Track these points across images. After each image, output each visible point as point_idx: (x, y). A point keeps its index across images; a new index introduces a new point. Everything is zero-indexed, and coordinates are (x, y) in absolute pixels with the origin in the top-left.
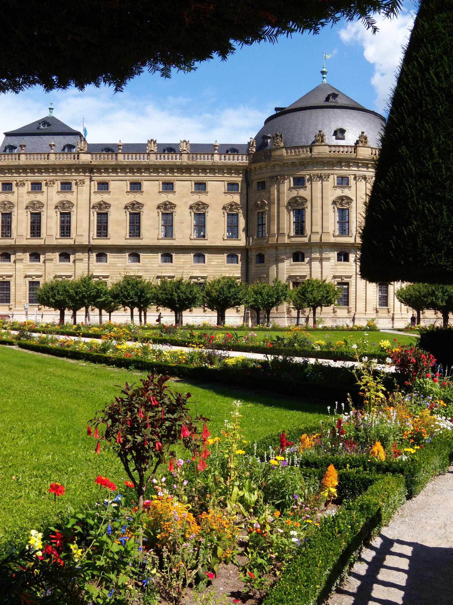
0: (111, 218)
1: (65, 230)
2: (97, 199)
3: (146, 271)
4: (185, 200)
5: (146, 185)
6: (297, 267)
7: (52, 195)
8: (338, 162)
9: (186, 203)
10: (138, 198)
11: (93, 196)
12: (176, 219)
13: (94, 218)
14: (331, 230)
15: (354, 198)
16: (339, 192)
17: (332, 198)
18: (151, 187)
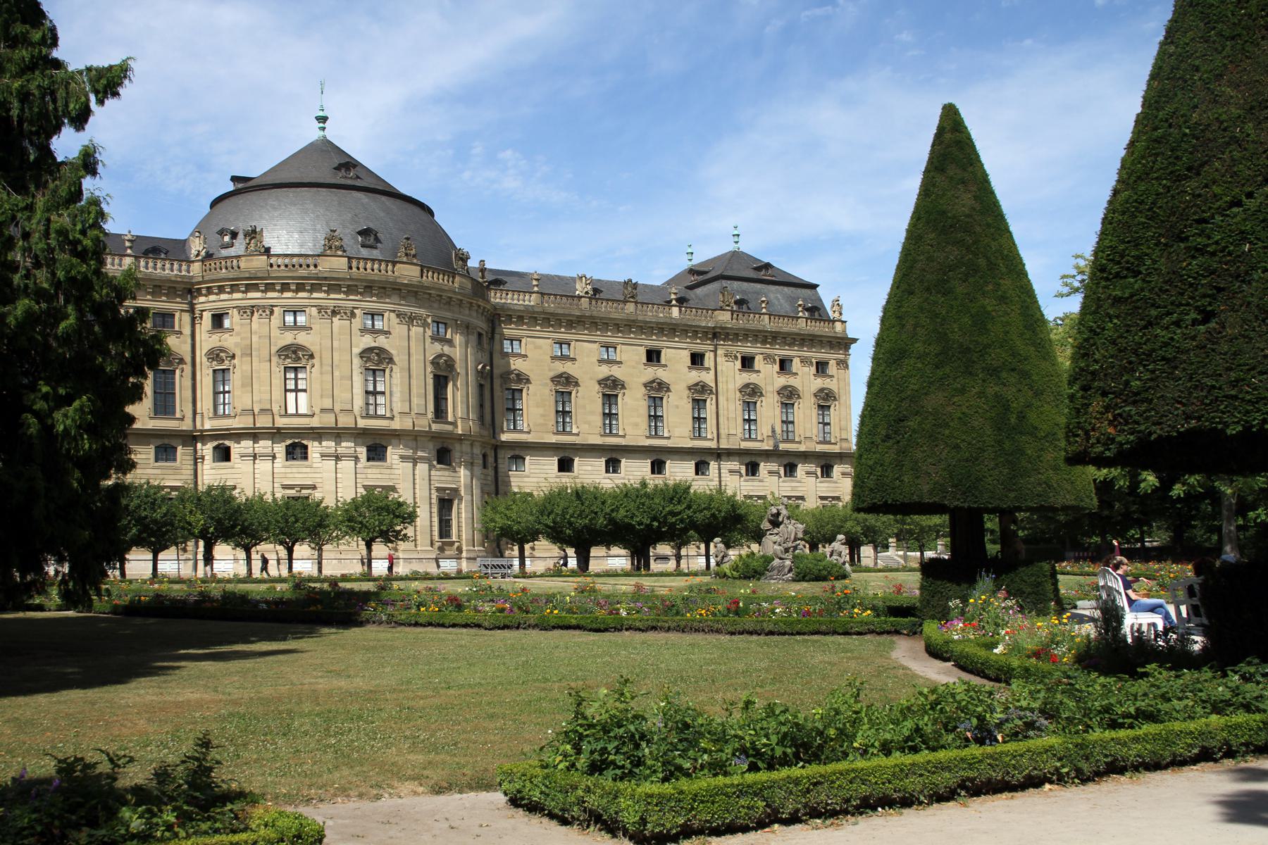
6: (294, 470)
8: (366, 287)
16: (368, 341)
17: (356, 351)
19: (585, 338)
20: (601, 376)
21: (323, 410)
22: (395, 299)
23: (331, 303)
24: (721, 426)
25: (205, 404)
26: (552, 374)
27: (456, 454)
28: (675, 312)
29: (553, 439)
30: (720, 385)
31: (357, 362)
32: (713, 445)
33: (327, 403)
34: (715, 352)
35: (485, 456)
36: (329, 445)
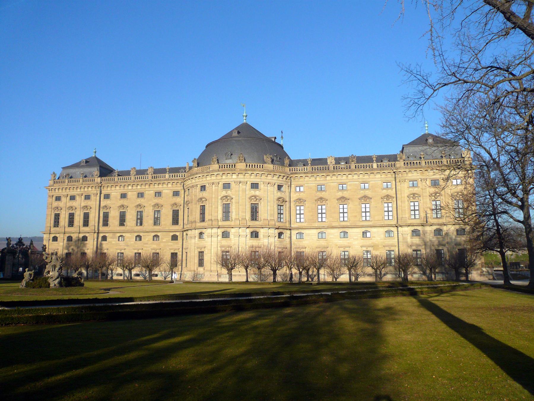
0: (111, 215)
1: (86, 223)
2: (104, 203)
3: (128, 246)
4: (150, 203)
5: (129, 194)
7: (79, 202)
9: (150, 204)
10: (124, 202)
11: (101, 203)
12: (144, 214)
13: (101, 215)
14: (219, 218)
15: (233, 197)
16: (224, 193)
17: (220, 197)
18: (132, 195)
19: (331, 181)
20: (339, 197)
21: (209, 220)
22: (234, 176)
23: (212, 181)
24: (399, 214)
25: (186, 221)
26: (316, 198)
27: (261, 235)
28: (375, 165)
29: (316, 225)
30: (398, 195)
31: (220, 201)
32: (394, 222)
33: (210, 218)
34: (395, 180)
35: (280, 234)
36: (209, 231)
